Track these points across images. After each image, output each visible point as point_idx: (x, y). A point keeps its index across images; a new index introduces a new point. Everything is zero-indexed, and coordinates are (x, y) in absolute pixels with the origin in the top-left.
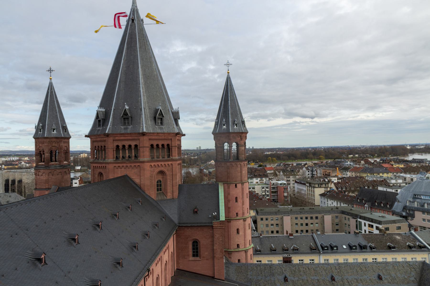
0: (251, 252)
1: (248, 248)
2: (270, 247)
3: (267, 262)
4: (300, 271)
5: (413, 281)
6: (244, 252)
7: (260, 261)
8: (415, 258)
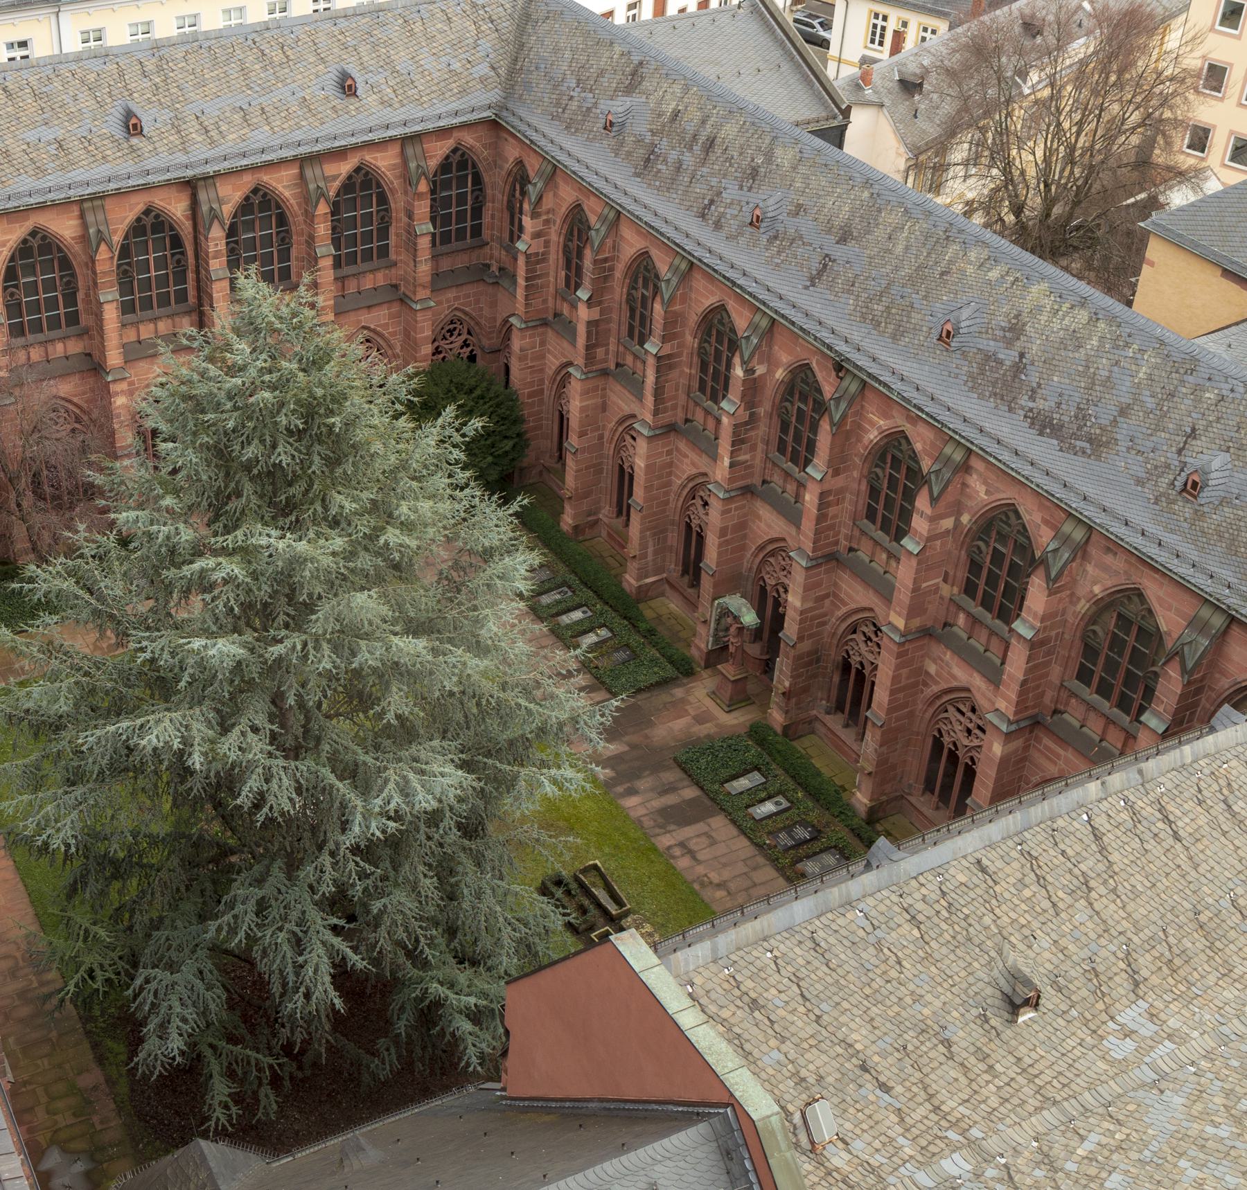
5: (483, 80)
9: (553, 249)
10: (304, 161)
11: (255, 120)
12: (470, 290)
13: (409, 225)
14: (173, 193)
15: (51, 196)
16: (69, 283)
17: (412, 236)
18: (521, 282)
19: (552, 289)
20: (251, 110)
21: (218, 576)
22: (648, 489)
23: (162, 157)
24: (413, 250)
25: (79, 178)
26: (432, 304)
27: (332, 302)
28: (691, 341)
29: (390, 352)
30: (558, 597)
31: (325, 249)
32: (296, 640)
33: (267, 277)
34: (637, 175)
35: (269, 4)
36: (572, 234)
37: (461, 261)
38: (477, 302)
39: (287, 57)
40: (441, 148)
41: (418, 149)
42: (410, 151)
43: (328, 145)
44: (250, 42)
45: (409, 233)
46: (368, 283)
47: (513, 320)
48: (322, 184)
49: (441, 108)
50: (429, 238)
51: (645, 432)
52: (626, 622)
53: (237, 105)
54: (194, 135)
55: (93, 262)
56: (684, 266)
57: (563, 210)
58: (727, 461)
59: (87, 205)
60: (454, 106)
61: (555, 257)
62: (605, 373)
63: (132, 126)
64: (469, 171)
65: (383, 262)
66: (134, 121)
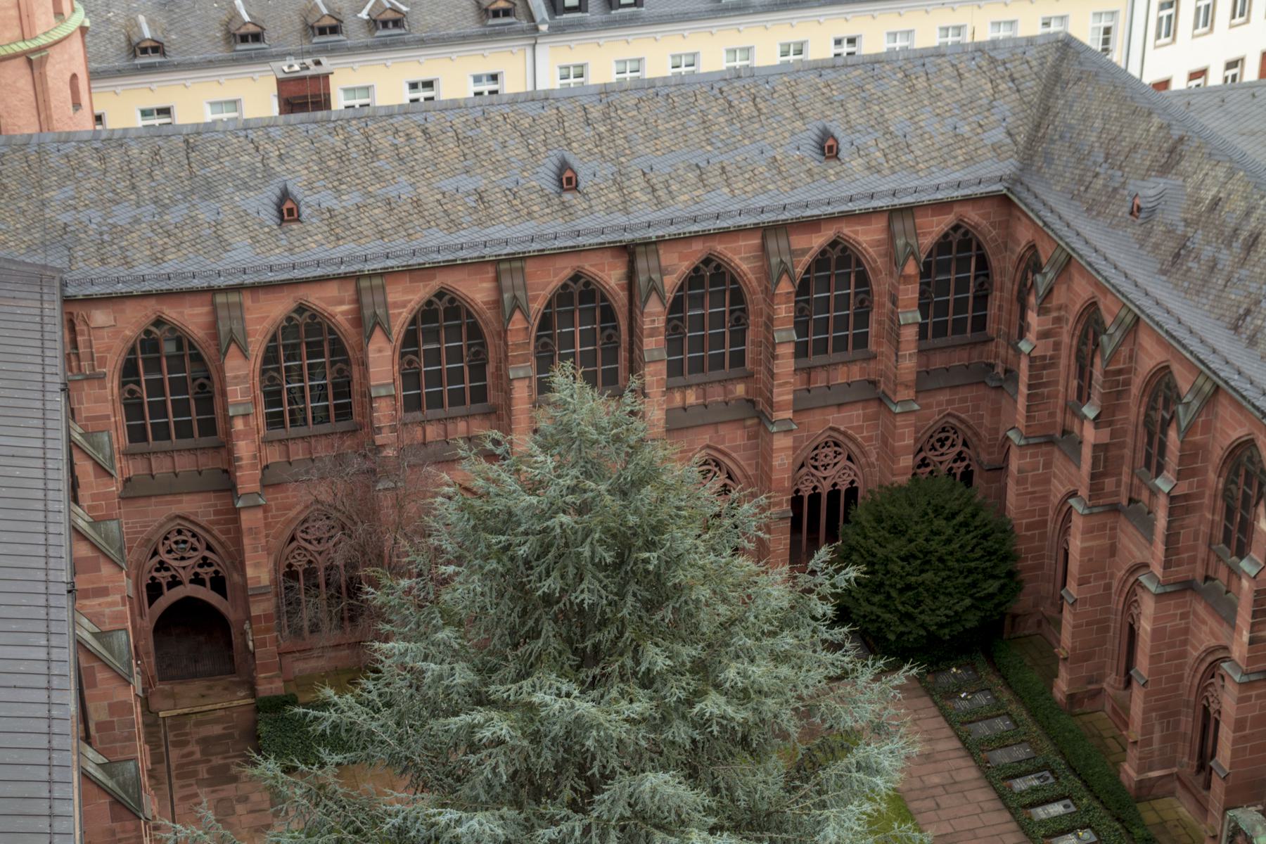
0: (68, 62)
1: (43, 41)
2: (225, 17)
3: (208, 116)
4: (376, 155)
5: (995, 148)
6: (21, 62)
7: (165, 111)
8: (1063, 18)
9: (1064, 353)
10: (768, 231)
11: (713, 181)
12: (969, 393)
13: (893, 312)
14: (607, 258)
15: (462, 254)
16: (477, 354)
17: (895, 327)
18: (1023, 389)
19: (1061, 402)
20: (709, 168)
21: (487, 733)
22: (1154, 659)
23: (599, 217)
24: (896, 343)
25: (498, 236)
26: (916, 407)
27: (791, 397)
28: (1214, 479)
29: (863, 460)
30: (1036, 783)
31: (785, 335)
32: (577, 823)
33: (590, 379)
34: (1164, 272)
35: (782, 45)
36: (1086, 336)
37: (959, 358)
38: (976, 408)
39: (759, 110)
40: (938, 225)
41: (909, 224)
42: (898, 226)
43: (798, 213)
44: (716, 91)
45: (892, 321)
46: (840, 376)
47: (1012, 434)
48: (786, 258)
49: (942, 180)
50: (915, 329)
51: (1153, 588)
52: (1117, 825)
53: (694, 161)
54: (638, 194)
55: (506, 331)
56: (1207, 388)
57: (1077, 307)
58: (1246, 636)
59: (503, 266)
60: (957, 176)
61: (1066, 361)
62: (1115, 509)
63: (567, 180)
64: (973, 253)
65: (860, 353)
66: (568, 174)
